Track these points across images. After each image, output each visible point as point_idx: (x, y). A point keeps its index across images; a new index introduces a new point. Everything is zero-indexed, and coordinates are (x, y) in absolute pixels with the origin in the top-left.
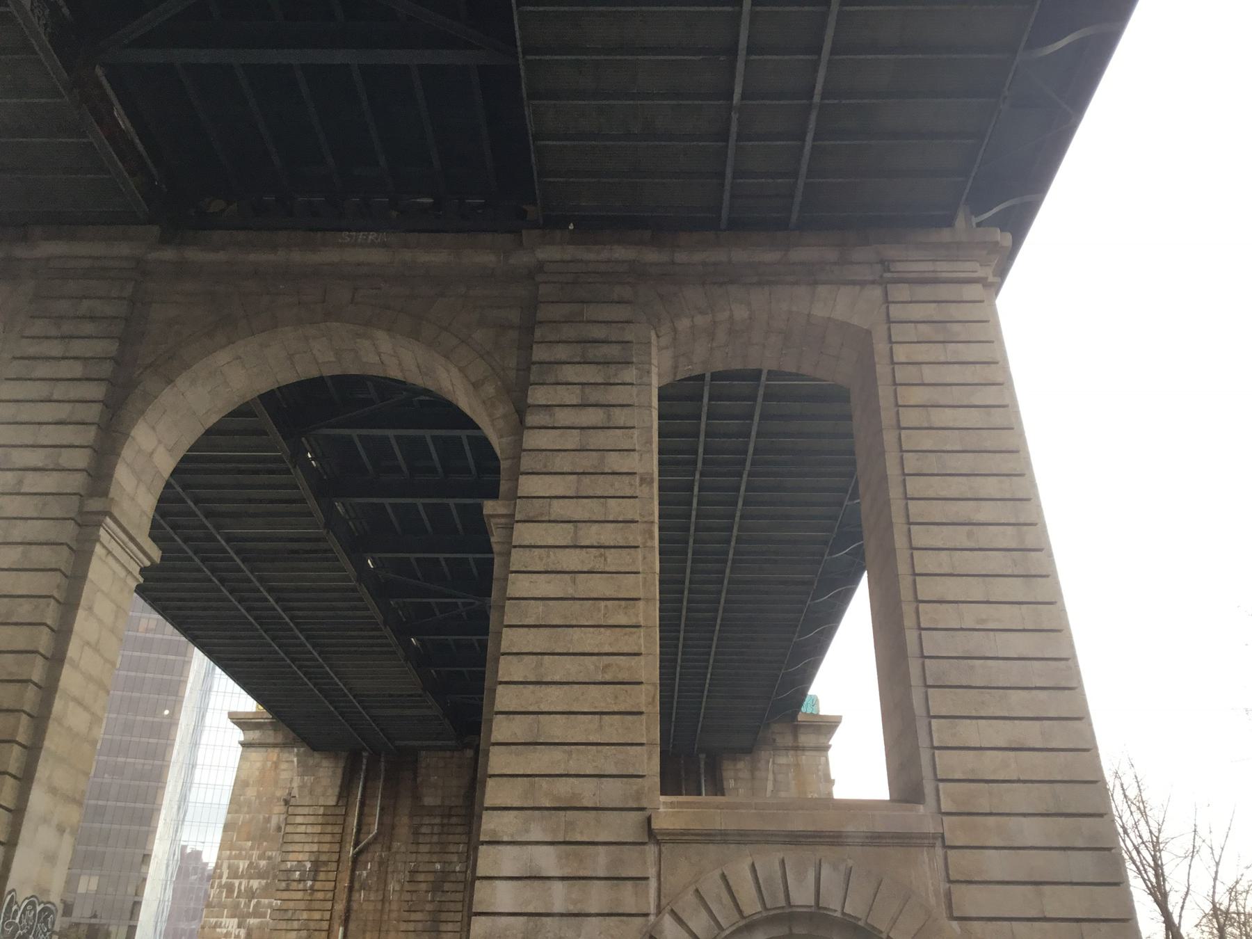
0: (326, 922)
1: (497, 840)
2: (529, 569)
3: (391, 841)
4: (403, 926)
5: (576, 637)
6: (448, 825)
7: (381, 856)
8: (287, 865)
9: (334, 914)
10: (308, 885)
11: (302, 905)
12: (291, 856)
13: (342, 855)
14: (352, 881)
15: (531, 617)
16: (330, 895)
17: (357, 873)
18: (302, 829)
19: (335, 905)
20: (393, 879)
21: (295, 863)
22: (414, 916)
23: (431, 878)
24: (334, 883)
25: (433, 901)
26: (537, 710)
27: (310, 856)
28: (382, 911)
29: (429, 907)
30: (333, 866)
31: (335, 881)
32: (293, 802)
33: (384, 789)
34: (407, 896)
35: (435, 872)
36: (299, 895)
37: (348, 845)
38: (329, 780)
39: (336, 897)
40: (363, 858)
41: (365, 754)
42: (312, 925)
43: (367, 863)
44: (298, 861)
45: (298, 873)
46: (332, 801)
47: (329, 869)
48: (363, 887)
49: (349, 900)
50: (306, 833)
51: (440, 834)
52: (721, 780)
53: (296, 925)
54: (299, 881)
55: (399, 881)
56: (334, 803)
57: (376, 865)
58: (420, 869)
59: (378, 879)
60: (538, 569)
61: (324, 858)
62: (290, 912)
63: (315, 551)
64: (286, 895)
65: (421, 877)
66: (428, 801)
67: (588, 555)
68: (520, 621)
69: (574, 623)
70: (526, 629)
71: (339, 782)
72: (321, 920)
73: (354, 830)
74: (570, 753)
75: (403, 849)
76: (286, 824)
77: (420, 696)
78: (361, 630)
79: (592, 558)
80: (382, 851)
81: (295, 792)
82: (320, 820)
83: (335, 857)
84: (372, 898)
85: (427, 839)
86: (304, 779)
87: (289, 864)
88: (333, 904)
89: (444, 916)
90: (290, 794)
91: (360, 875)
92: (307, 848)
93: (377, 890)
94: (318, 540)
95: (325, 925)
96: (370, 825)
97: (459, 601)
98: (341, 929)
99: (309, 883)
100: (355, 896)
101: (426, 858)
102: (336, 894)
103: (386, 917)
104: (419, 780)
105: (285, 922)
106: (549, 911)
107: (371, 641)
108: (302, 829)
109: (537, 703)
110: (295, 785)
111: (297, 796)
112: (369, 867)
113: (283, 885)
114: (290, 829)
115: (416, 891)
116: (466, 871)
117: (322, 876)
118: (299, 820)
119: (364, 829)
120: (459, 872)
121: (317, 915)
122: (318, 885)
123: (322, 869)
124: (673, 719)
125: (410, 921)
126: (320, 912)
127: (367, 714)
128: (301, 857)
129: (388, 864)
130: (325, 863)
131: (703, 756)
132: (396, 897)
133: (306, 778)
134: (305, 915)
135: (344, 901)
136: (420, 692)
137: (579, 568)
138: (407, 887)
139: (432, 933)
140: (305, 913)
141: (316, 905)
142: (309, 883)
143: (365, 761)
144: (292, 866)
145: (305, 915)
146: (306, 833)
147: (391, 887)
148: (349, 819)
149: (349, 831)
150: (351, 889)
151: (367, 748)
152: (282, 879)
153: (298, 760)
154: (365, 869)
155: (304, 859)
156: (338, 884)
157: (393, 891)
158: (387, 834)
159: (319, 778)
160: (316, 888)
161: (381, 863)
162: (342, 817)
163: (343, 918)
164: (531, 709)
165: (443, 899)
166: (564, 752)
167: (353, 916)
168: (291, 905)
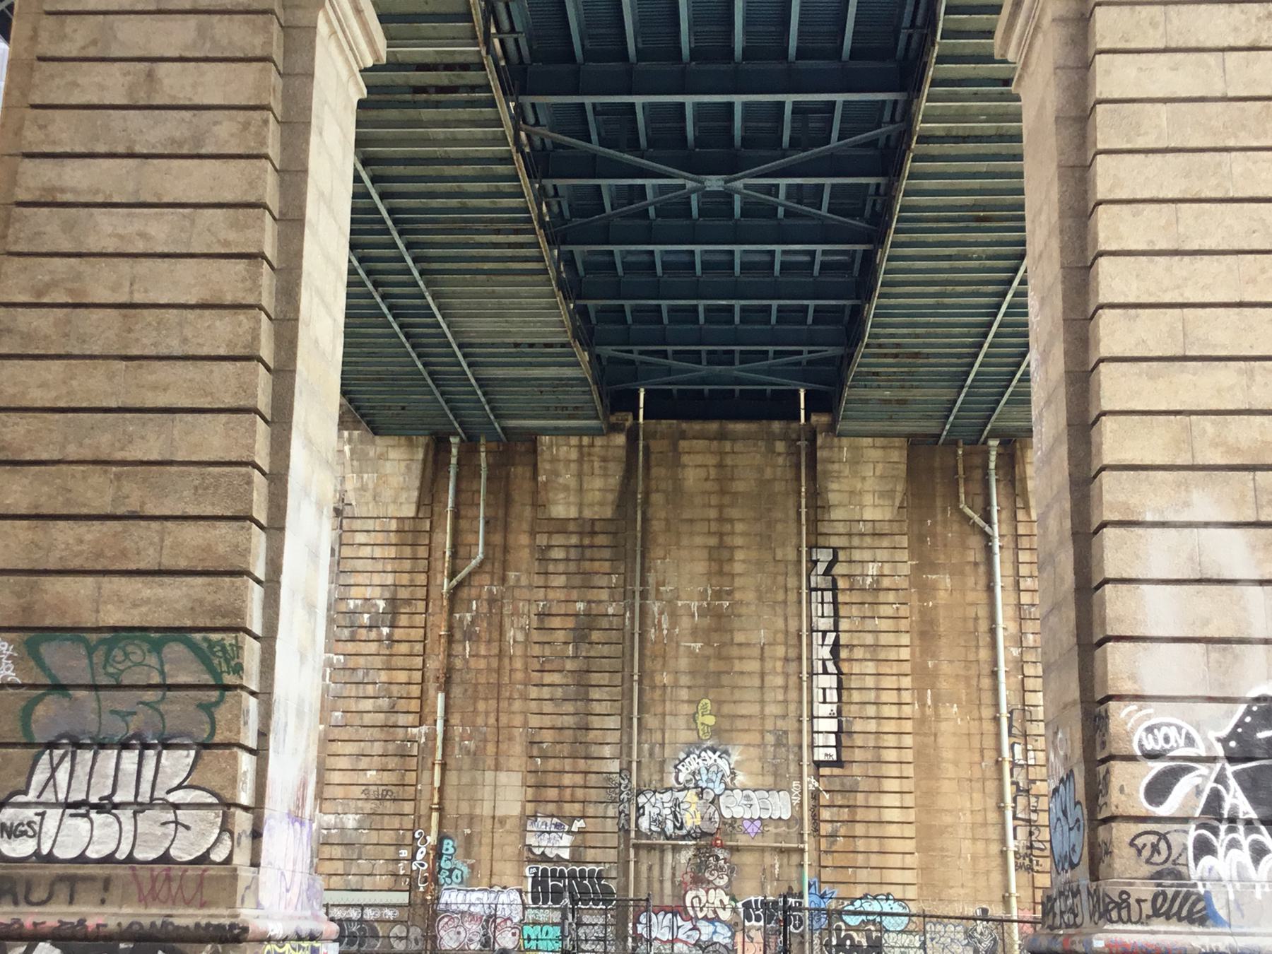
0: (415, 686)
1: (1134, 518)
2: (1133, 45)
3: (505, 566)
4: (534, 692)
5: (1237, 169)
6: (592, 546)
7: (490, 591)
8: (348, 604)
9: (427, 674)
10: (385, 633)
11: (378, 662)
12: (354, 592)
13: (432, 589)
14: (450, 628)
15: (1146, 133)
16: (418, 648)
17: (457, 616)
18: (366, 551)
19: (427, 661)
20: (512, 626)
21: (359, 602)
22: (548, 678)
23: (570, 622)
24: (422, 630)
25: (576, 657)
26: (1180, 300)
27: (383, 591)
28: (499, 671)
29: (569, 665)
30: (421, 606)
31: (425, 627)
32: (348, 511)
33: (488, 491)
34: (536, 650)
35: (576, 615)
36: (373, 647)
37: (439, 576)
38: (401, 479)
39: (428, 651)
40: (464, 593)
41: (454, 440)
42: (395, 690)
43: (470, 601)
44: (366, 599)
45: (366, 616)
46: (409, 511)
47: (414, 611)
48: (470, 636)
49: (449, 655)
50: (372, 558)
51: (579, 560)
52: (1024, 480)
53: (370, 690)
54: (370, 627)
55: (522, 628)
56: (412, 514)
57: (485, 604)
58: (554, 611)
59: (489, 624)
60: (1150, 45)
61: (403, 594)
62: (360, 673)
63: (454, 89)
64: (350, 647)
65: (556, 622)
66: (562, 509)
67: (1243, 17)
68: (1128, 142)
69: (1231, 143)
70: (1142, 156)
71: (417, 483)
72: (409, 684)
73: (448, 554)
74: (1251, 374)
75: (524, 581)
76: (341, 545)
77: (563, 345)
78: (498, 232)
79: (1254, 21)
80: (492, 584)
81: (351, 497)
82: (393, 538)
83: (421, 593)
84: (483, 652)
85: (561, 567)
86: (362, 478)
87: (351, 604)
88: (424, 660)
89: (595, 678)
90: (343, 500)
91: (461, 620)
92: (377, 579)
93: (489, 642)
94: (465, 67)
95: (415, 691)
96: (470, 546)
97: (649, 182)
98: (441, 697)
99: (385, 630)
100: (457, 648)
101: (561, 595)
102: (428, 646)
103: (506, 680)
104: (542, 478)
105: (354, 686)
106: (1245, 636)
107: (509, 252)
108: (366, 551)
109: (1178, 287)
110: (351, 484)
111: (354, 503)
112: (474, 607)
113: (346, 633)
114: (346, 552)
115: (549, 643)
116: (624, 615)
117: (403, 620)
118: (361, 538)
119: (462, 551)
120: (613, 615)
121: (402, 676)
122: (398, 634)
123: (403, 610)
124: (969, 382)
125: (543, 685)
126: (406, 672)
127: (473, 375)
128: (368, 592)
129: (502, 603)
130: (408, 601)
131: (994, 443)
132: (519, 653)
133: (365, 476)
134: (383, 677)
135: (441, 657)
136: (568, 338)
137: (1231, 41)
138: (536, 636)
139: (579, 703)
140: (383, 673)
141: (400, 662)
142: (385, 630)
143: (454, 451)
144: (356, 606)
145: (383, 677)
146: (372, 558)
147: (511, 634)
148: (437, 537)
149: (438, 554)
150: (450, 639)
151: (460, 430)
152: (343, 624)
153: (352, 451)
154: (469, 610)
155: (374, 596)
156: (428, 630)
157: (515, 641)
158: (499, 558)
159: (386, 475)
160: (396, 637)
161: (492, 601)
162: (427, 535)
163: (442, 680)
164: (1167, 299)
165: (592, 654)
166: (1240, 372)
167: (456, 677)
168: (361, 661)
